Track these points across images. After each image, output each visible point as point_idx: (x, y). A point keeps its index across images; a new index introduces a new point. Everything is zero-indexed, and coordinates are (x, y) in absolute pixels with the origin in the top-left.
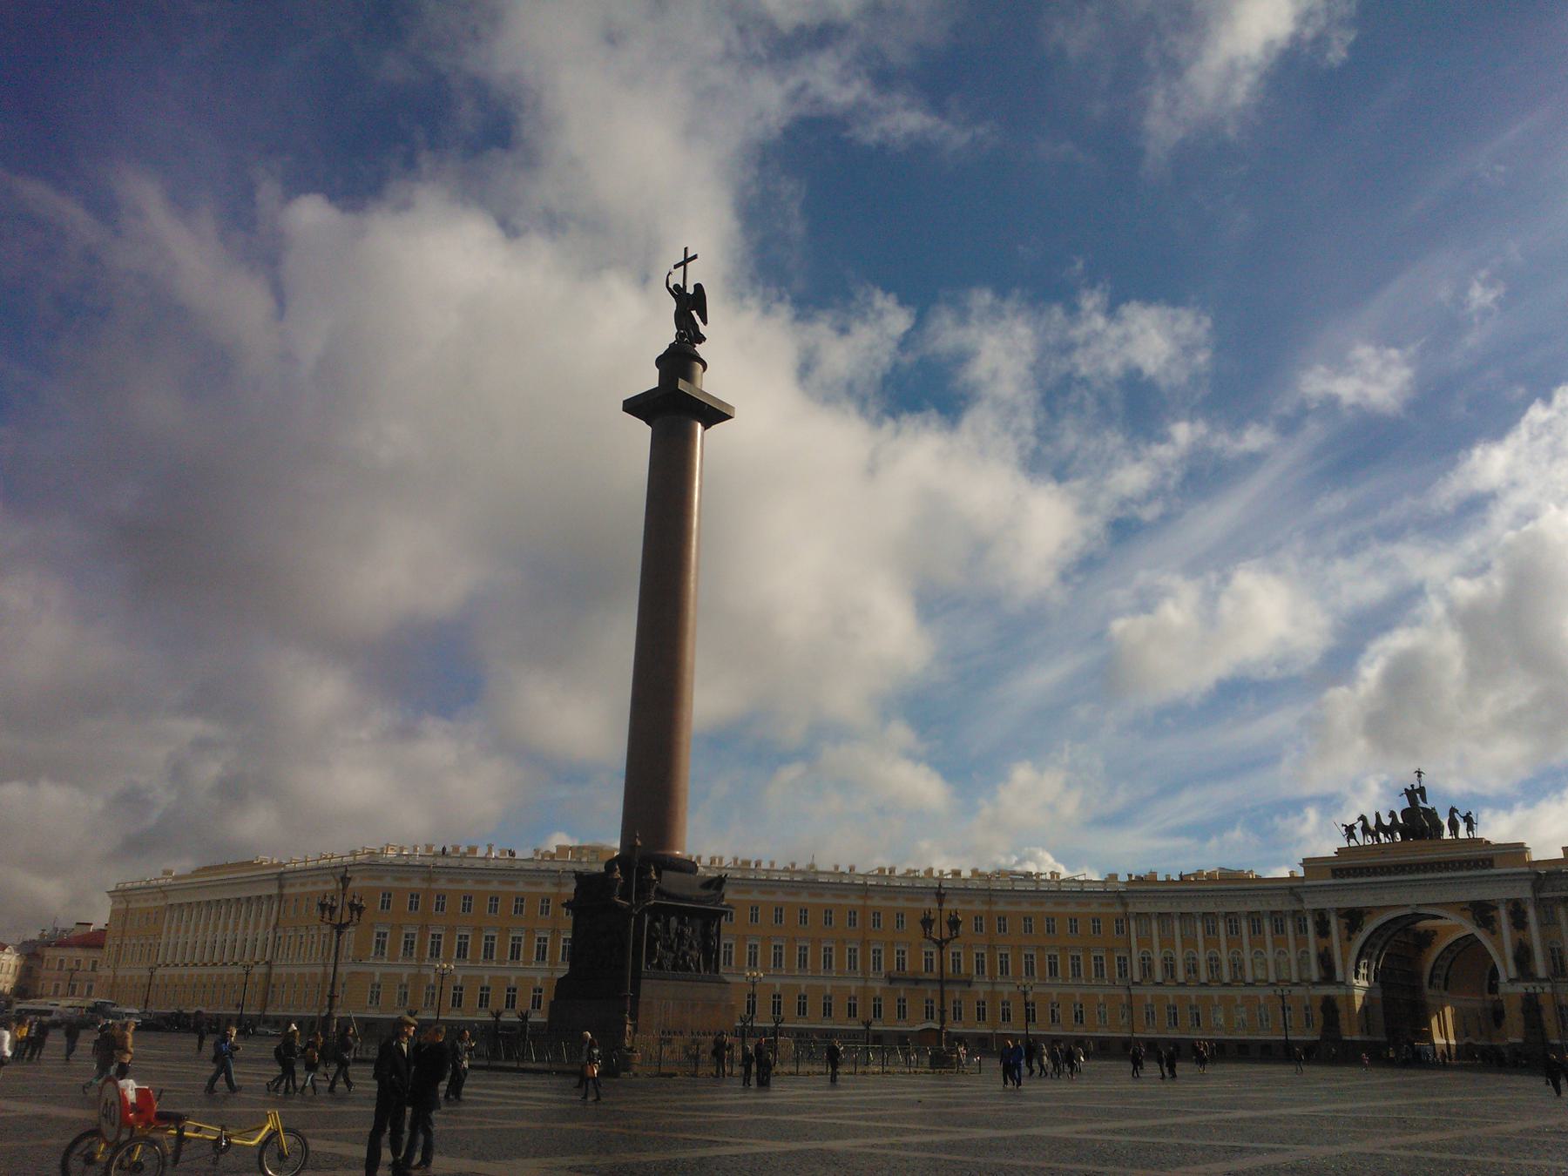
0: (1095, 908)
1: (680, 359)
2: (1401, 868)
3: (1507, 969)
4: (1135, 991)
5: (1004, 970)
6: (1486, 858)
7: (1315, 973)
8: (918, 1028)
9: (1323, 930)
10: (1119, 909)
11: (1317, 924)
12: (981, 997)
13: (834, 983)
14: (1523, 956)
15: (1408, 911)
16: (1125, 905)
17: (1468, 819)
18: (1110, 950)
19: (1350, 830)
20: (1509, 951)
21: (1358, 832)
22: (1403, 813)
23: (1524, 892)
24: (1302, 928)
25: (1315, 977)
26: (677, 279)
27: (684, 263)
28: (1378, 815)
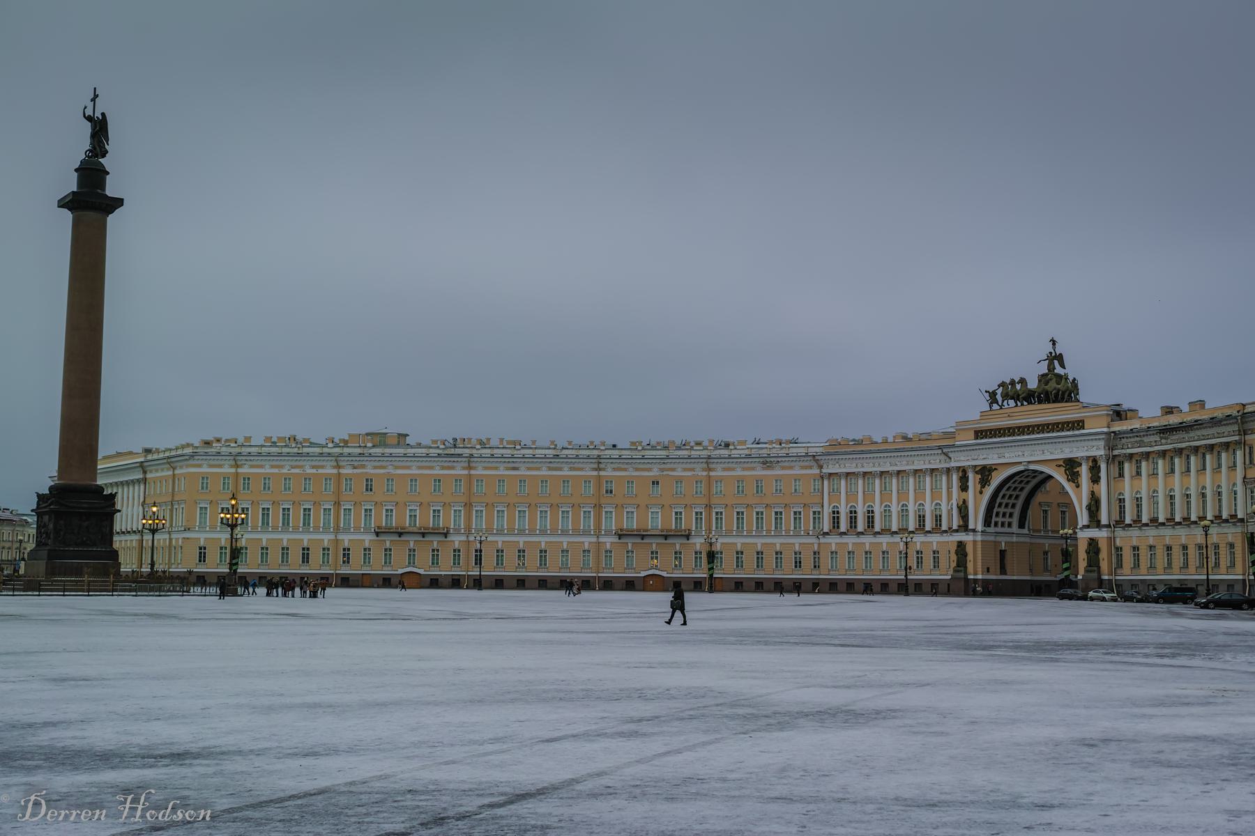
2: (1010, 431)
3: (1083, 518)
4: (823, 540)
12: (698, 548)
13: (572, 539)
14: (1094, 506)
15: (1021, 468)
16: (821, 467)
19: (993, 395)
20: (1085, 502)
21: (999, 397)
22: (1043, 378)
23: (1099, 450)
25: (955, 527)
26: (89, 112)
27: (93, 100)
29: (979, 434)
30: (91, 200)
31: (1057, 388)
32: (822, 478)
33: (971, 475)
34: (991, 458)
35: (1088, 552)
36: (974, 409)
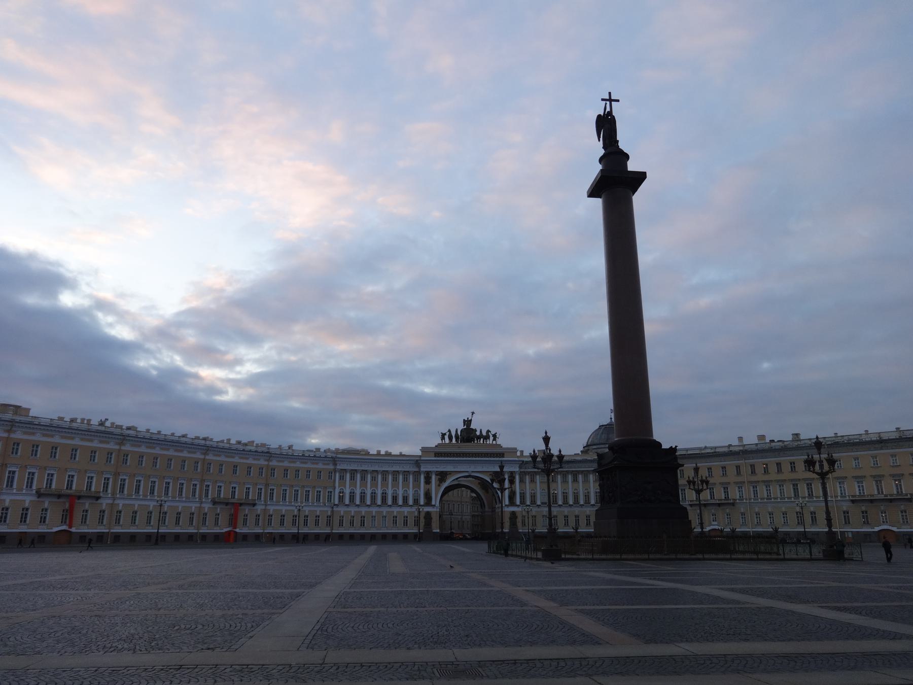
0: (320, 466)
1: (614, 156)
5: (271, 498)
6: (499, 453)
7: (422, 502)
8: (225, 530)
9: (428, 481)
10: (331, 467)
11: (425, 478)
16: (335, 464)
17: (495, 436)
18: (326, 488)
19: (443, 435)
21: (446, 437)
24: (417, 480)
25: (422, 502)
28: (457, 431)
29: (437, 454)
30: (616, 183)
31: (468, 434)
32: (335, 472)
33: (434, 477)
34: (449, 468)
35: (510, 519)
36: (434, 441)
